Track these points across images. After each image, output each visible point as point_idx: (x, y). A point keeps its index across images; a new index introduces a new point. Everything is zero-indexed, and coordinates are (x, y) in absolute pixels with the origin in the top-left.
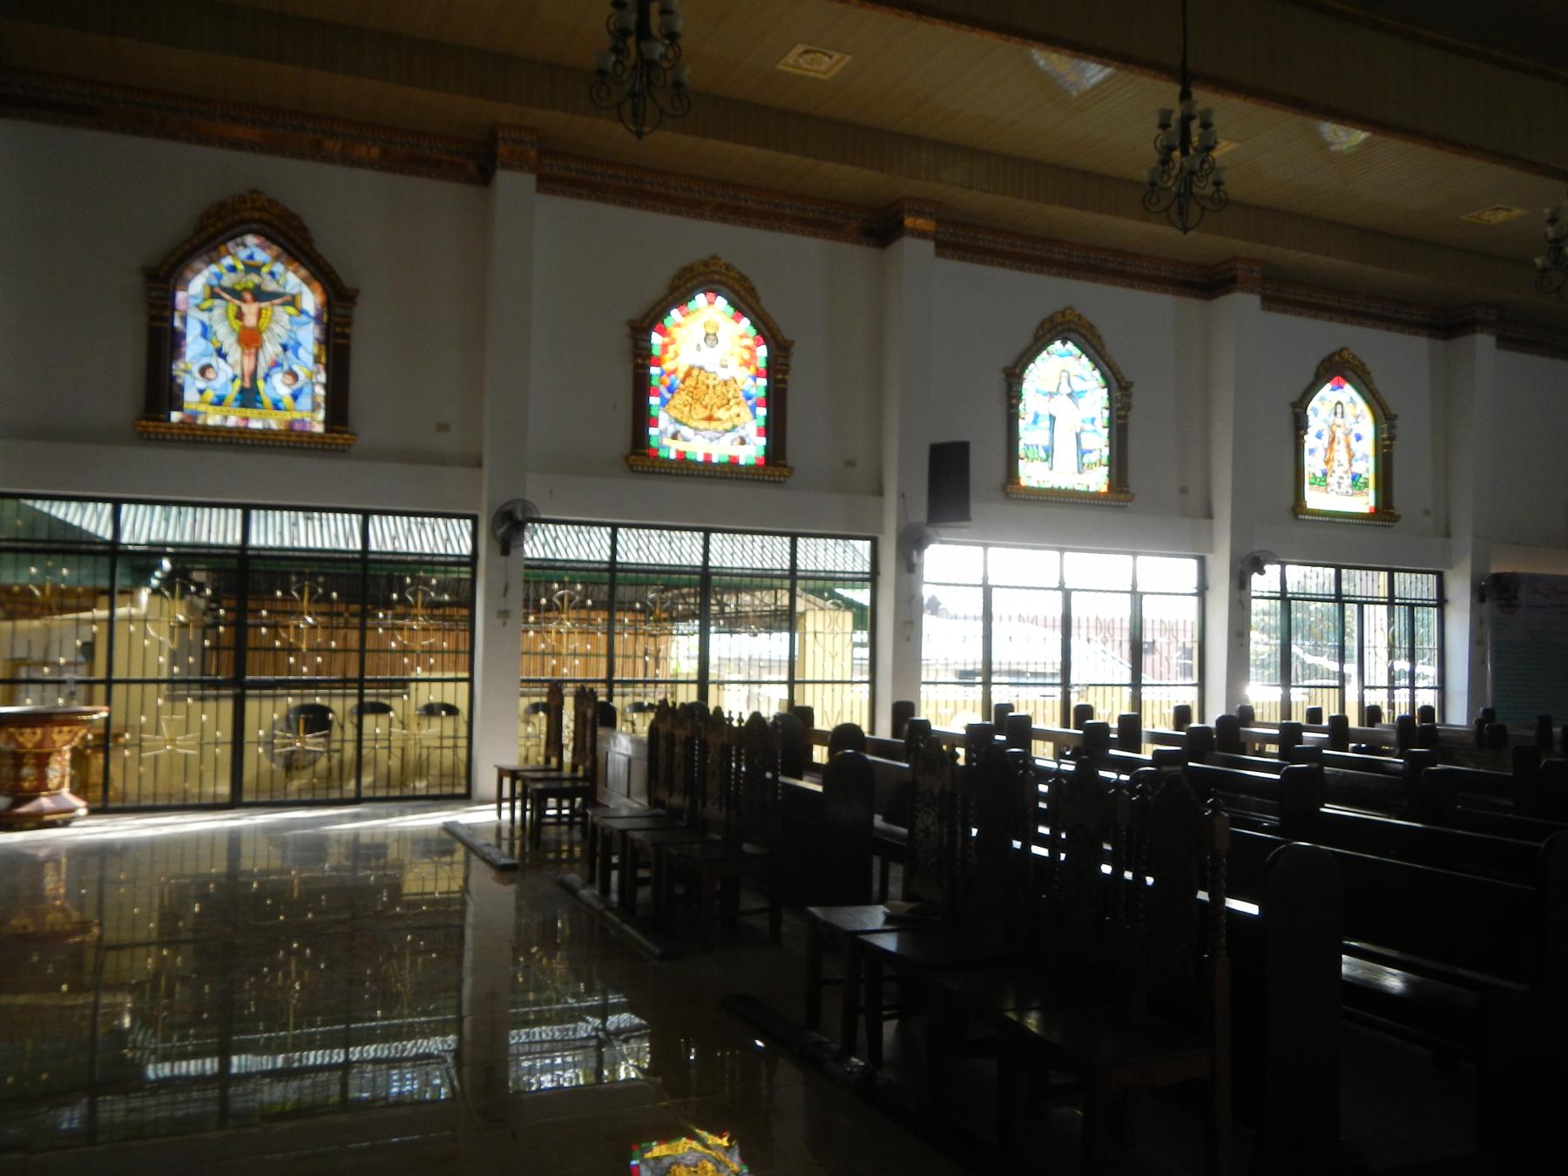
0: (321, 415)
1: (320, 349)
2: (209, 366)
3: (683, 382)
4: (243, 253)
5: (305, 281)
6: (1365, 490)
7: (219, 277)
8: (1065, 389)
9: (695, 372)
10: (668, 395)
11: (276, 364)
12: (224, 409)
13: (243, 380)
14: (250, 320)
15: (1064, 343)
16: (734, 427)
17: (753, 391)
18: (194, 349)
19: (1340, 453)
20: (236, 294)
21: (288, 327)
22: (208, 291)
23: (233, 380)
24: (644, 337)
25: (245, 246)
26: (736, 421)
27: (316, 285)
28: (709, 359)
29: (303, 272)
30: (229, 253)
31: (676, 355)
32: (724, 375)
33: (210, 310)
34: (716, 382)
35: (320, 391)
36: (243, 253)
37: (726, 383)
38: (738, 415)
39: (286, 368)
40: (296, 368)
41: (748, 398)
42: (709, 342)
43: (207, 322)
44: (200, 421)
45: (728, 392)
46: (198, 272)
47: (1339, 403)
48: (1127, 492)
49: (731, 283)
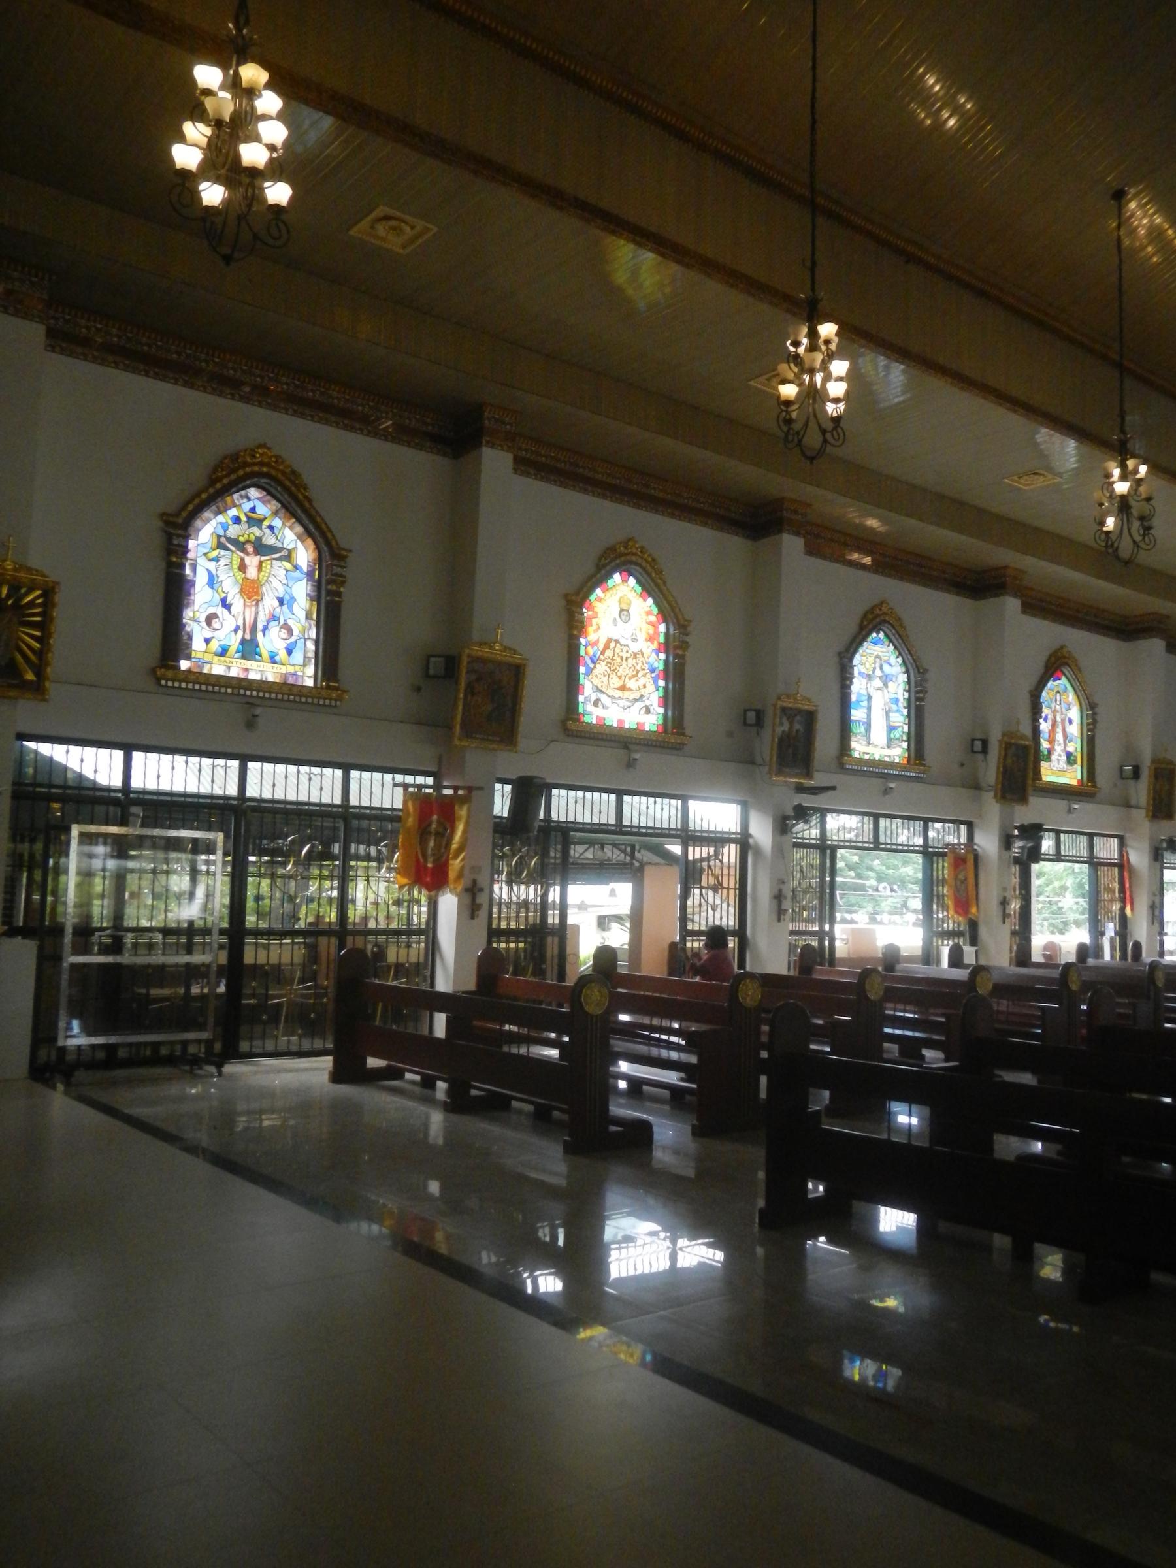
0: (310, 670)
1: (311, 605)
3: (603, 653)
5: (299, 537)
6: (1075, 766)
7: (225, 527)
8: (878, 673)
9: (612, 645)
10: (592, 665)
11: (274, 618)
12: (228, 659)
13: (244, 631)
14: (252, 573)
15: (878, 633)
16: (642, 696)
17: (656, 665)
18: (201, 600)
19: (1059, 737)
20: (240, 545)
21: (285, 582)
23: (236, 631)
24: (578, 610)
25: (249, 499)
26: (643, 691)
27: (310, 541)
28: (621, 631)
29: (299, 529)
30: (235, 506)
31: (599, 628)
32: (635, 648)
34: (629, 655)
35: (311, 646)
36: (247, 506)
37: (635, 655)
38: (645, 686)
39: (282, 622)
40: (290, 622)
41: (653, 671)
42: (623, 617)
43: (214, 572)
44: (205, 671)
45: (637, 664)
46: (208, 521)
47: (1058, 692)
48: (924, 765)
49: (644, 564)
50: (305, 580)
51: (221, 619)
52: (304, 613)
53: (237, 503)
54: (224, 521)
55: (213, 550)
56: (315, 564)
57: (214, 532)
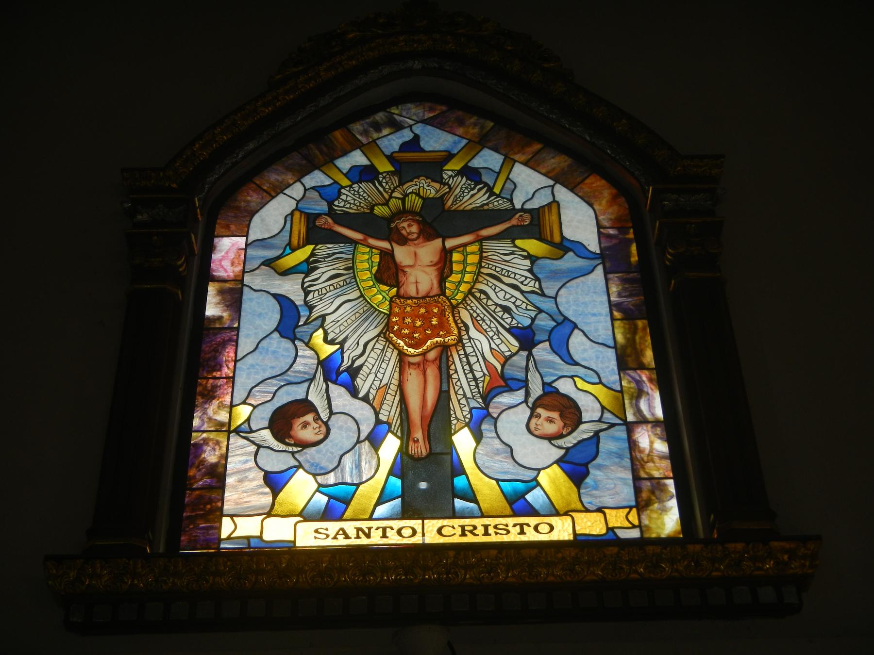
1: (632, 331)
2: (304, 406)
4: (392, 142)
5: (560, 178)
7: (330, 194)
13: (406, 436)
21: (532, 286)
22: (300, 227)
23: (375, 440)
30: (358, 145)
33: (309, 267)
36: (392, 142)
39: (537, 390)
40: (565, 387)
43: (298, 298)
46: (279, 189)
50: (599, 271)
51: (324, 415)
52: (611, 354)
53: (364, 140)
54: (328, 182)
55: (293, 250)
56: (622, 230)
57: (297, 209)
